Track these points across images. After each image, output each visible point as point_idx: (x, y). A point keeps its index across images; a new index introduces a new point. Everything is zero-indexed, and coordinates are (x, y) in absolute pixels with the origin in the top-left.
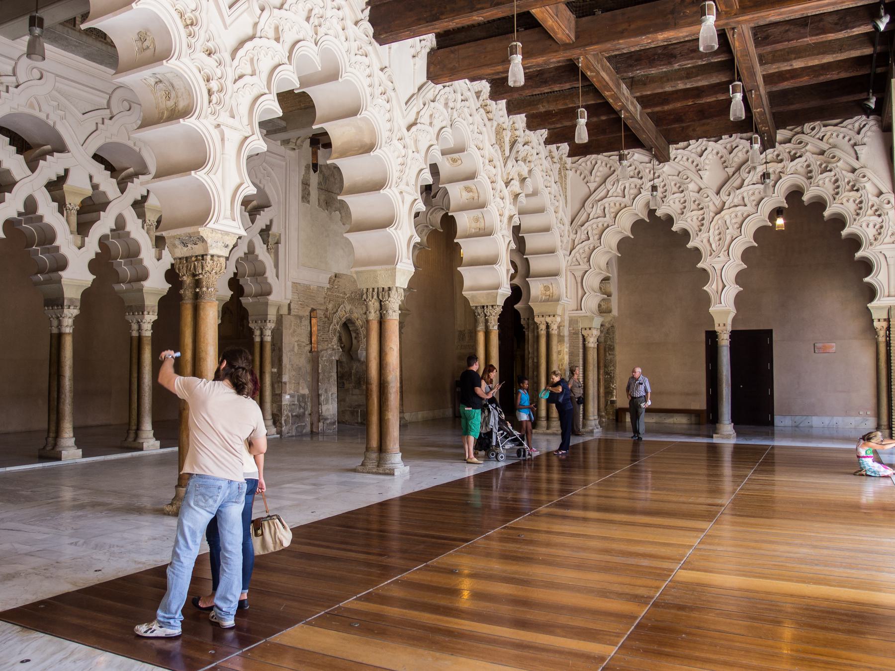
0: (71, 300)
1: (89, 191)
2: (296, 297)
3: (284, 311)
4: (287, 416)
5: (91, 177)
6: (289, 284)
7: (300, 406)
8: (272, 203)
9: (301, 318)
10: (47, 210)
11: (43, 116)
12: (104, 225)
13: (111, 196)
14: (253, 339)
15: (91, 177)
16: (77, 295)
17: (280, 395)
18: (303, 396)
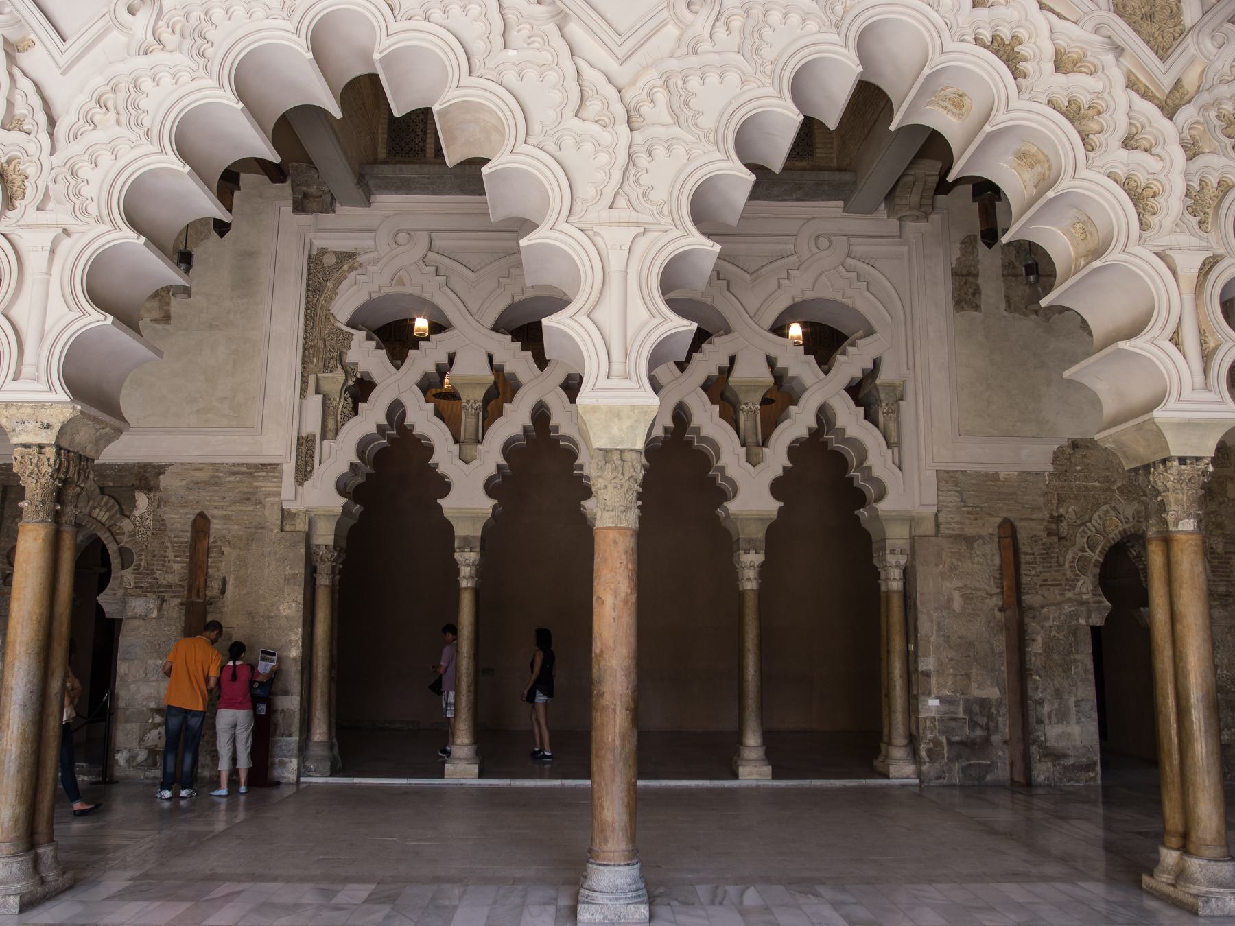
0: (466, 541)
1: (490, 378)
2: (954, 499)
3: (929, 528)
4: (936, 742)
5: (490, 357)
6: (930, 475)
7: (973, 724)
8: (876, 327)
9: (970, 540)
10: (423, 418)
12: (798, 423)
13: (522, 377)
14: (879, 586)
15: (490, 357)
16: (476, 531)
17: (916, 698)
18: (984, 703)
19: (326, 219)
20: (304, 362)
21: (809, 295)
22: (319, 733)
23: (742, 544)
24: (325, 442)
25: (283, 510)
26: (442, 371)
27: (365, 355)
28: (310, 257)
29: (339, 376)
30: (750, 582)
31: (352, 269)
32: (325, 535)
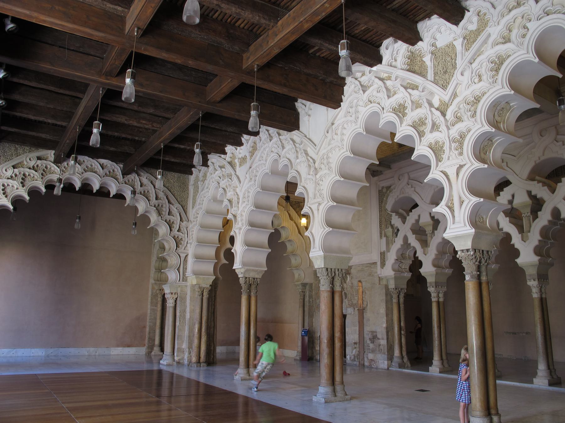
0: (430, 283)
1: (432, 222)
11: (407, 195)
19: (382, 177)
20: (380, 227)
21: (543, 158)
22: (397, 353)
23: (528, 277)
24: (388, 253)
25: (379, 277)
26: (418, 221)
27: (396, 221)
28: (379, 191)
29: (390, 229)
30: (535, 295)
31: (390, 192)
32: (392, 285)
